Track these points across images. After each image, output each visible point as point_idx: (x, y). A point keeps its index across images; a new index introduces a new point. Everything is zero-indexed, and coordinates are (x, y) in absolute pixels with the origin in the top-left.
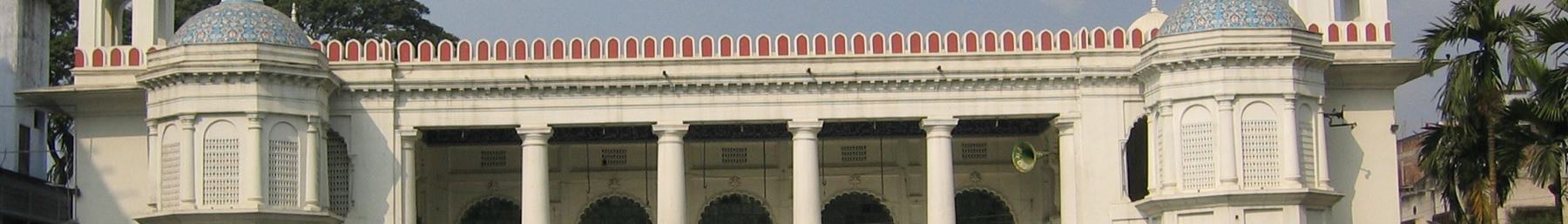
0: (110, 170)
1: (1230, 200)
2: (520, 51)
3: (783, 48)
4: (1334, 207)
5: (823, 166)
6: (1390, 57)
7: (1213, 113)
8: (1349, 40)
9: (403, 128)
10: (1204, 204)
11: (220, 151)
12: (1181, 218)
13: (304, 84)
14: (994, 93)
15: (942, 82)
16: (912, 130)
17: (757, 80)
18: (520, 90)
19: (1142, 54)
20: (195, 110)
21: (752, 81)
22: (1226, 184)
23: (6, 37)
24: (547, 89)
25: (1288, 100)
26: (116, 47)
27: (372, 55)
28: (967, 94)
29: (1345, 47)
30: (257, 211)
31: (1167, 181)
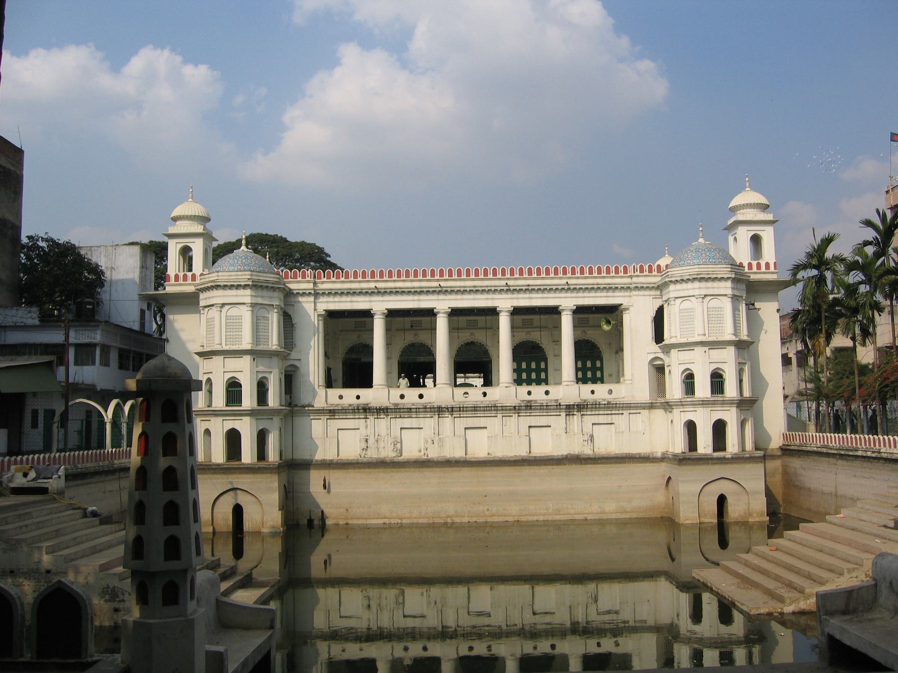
0: (182, 330)
1: (702, 344)
2: (373, 274)
3: (495, 274)
4: (750, 347)
5: (513, 328)
6: (776, 277)
7: (694, 303)
8: (757, 269)
9: (318, 311)
10: (690, 345)
11: (233, 321)
12: (679, 352)
13: (272, 290)
14: (592, 294)
15: (569, 289)
16: (554, 311)
17: (483, 288)
19: (661, 276)
21: (480, 289)
22: (700, 336)
23: (134, 268)
24: (385, 292)
25: (729, 297)
26: (185, 273)
27: (304, 276)
28: (580, 294)
29: (755, 273)
30: (250, 349)
31: (673, 335)
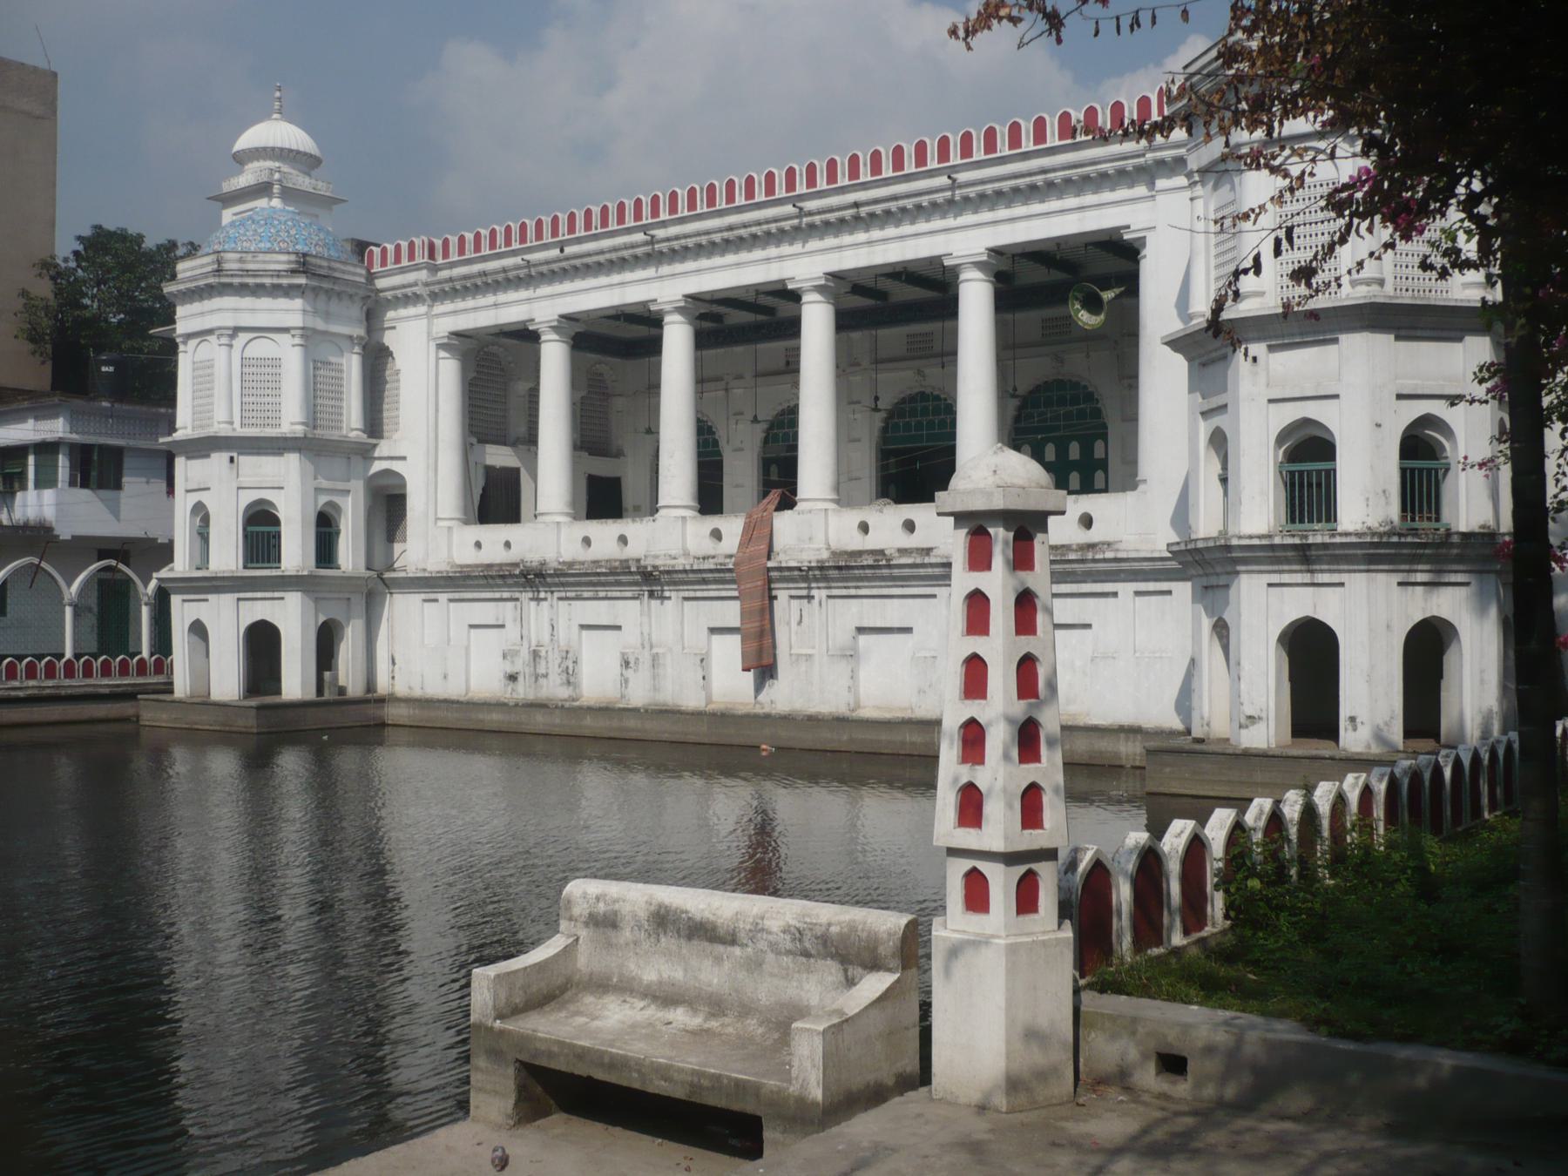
20: (231, 324)
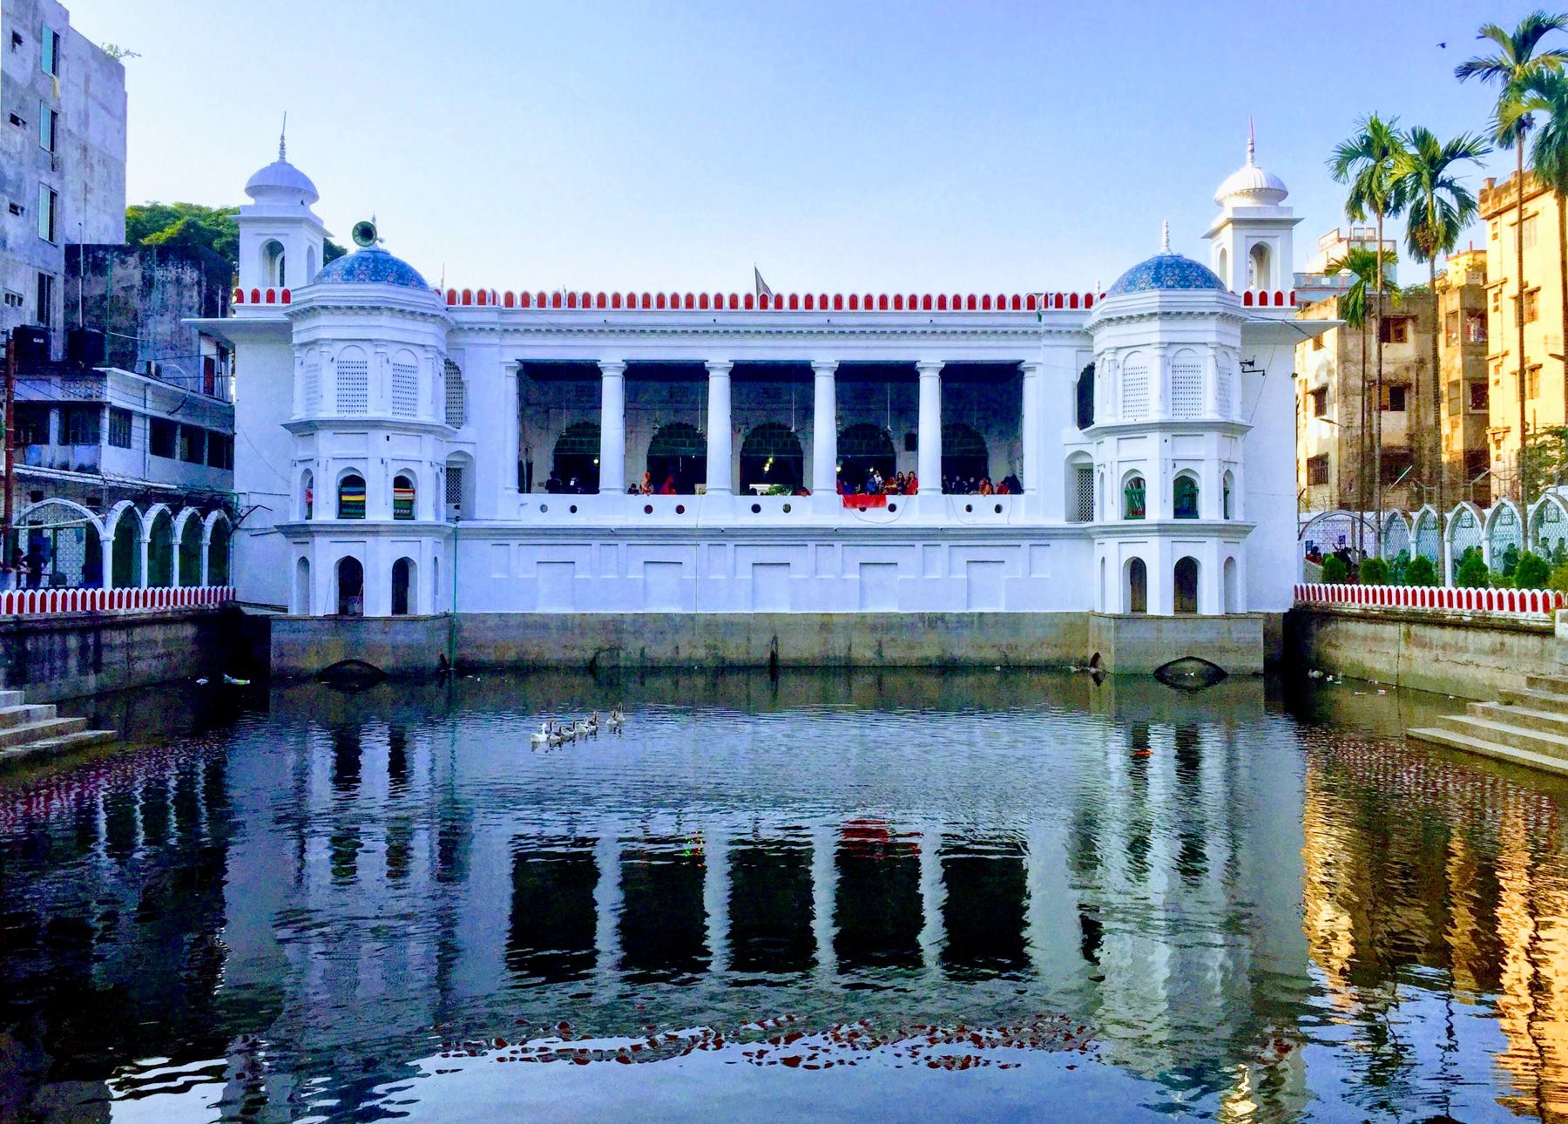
1: (1163, 426)
5: (840, 398)
8: (1261, 304)
18: (601, 331)
